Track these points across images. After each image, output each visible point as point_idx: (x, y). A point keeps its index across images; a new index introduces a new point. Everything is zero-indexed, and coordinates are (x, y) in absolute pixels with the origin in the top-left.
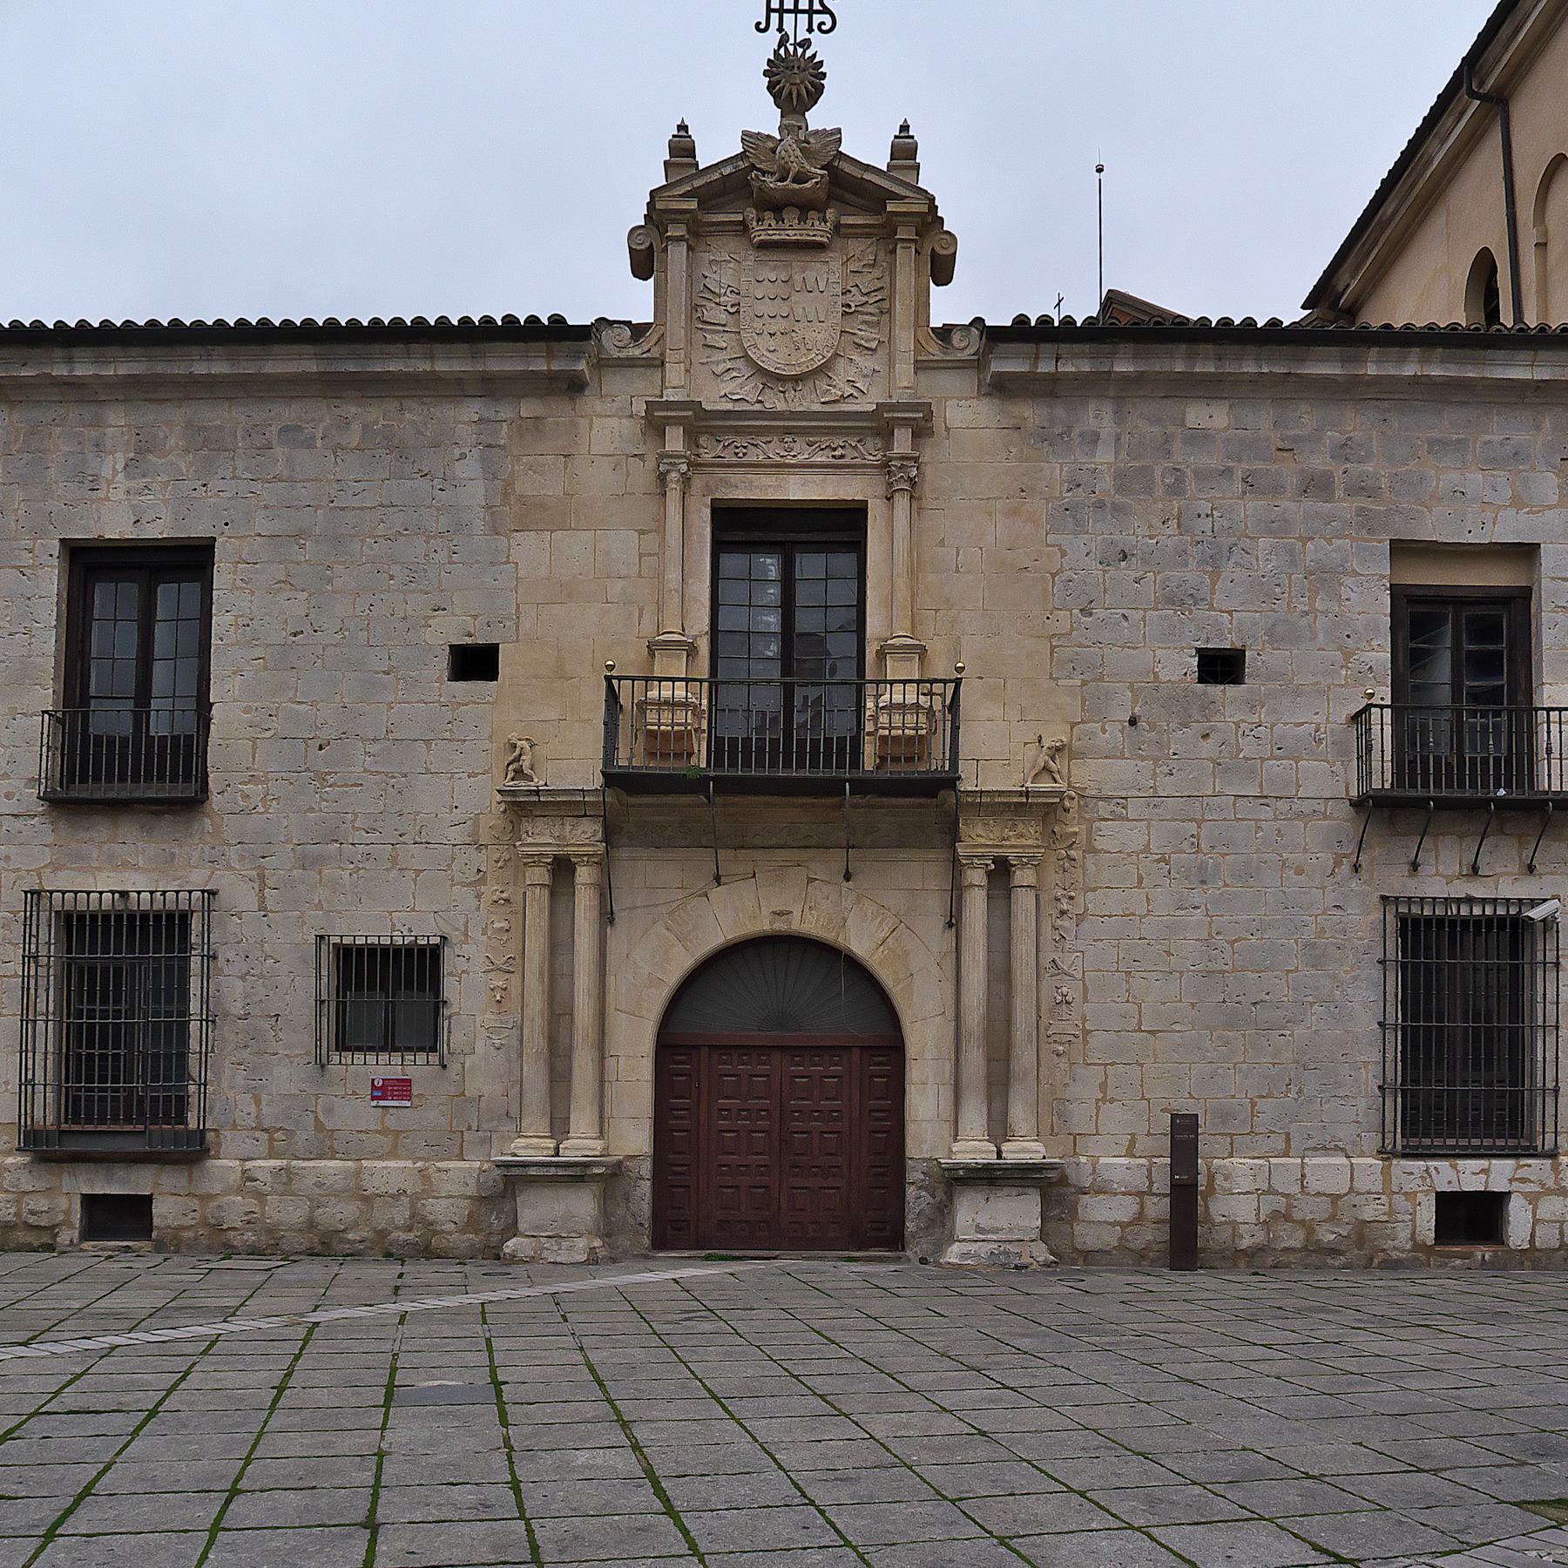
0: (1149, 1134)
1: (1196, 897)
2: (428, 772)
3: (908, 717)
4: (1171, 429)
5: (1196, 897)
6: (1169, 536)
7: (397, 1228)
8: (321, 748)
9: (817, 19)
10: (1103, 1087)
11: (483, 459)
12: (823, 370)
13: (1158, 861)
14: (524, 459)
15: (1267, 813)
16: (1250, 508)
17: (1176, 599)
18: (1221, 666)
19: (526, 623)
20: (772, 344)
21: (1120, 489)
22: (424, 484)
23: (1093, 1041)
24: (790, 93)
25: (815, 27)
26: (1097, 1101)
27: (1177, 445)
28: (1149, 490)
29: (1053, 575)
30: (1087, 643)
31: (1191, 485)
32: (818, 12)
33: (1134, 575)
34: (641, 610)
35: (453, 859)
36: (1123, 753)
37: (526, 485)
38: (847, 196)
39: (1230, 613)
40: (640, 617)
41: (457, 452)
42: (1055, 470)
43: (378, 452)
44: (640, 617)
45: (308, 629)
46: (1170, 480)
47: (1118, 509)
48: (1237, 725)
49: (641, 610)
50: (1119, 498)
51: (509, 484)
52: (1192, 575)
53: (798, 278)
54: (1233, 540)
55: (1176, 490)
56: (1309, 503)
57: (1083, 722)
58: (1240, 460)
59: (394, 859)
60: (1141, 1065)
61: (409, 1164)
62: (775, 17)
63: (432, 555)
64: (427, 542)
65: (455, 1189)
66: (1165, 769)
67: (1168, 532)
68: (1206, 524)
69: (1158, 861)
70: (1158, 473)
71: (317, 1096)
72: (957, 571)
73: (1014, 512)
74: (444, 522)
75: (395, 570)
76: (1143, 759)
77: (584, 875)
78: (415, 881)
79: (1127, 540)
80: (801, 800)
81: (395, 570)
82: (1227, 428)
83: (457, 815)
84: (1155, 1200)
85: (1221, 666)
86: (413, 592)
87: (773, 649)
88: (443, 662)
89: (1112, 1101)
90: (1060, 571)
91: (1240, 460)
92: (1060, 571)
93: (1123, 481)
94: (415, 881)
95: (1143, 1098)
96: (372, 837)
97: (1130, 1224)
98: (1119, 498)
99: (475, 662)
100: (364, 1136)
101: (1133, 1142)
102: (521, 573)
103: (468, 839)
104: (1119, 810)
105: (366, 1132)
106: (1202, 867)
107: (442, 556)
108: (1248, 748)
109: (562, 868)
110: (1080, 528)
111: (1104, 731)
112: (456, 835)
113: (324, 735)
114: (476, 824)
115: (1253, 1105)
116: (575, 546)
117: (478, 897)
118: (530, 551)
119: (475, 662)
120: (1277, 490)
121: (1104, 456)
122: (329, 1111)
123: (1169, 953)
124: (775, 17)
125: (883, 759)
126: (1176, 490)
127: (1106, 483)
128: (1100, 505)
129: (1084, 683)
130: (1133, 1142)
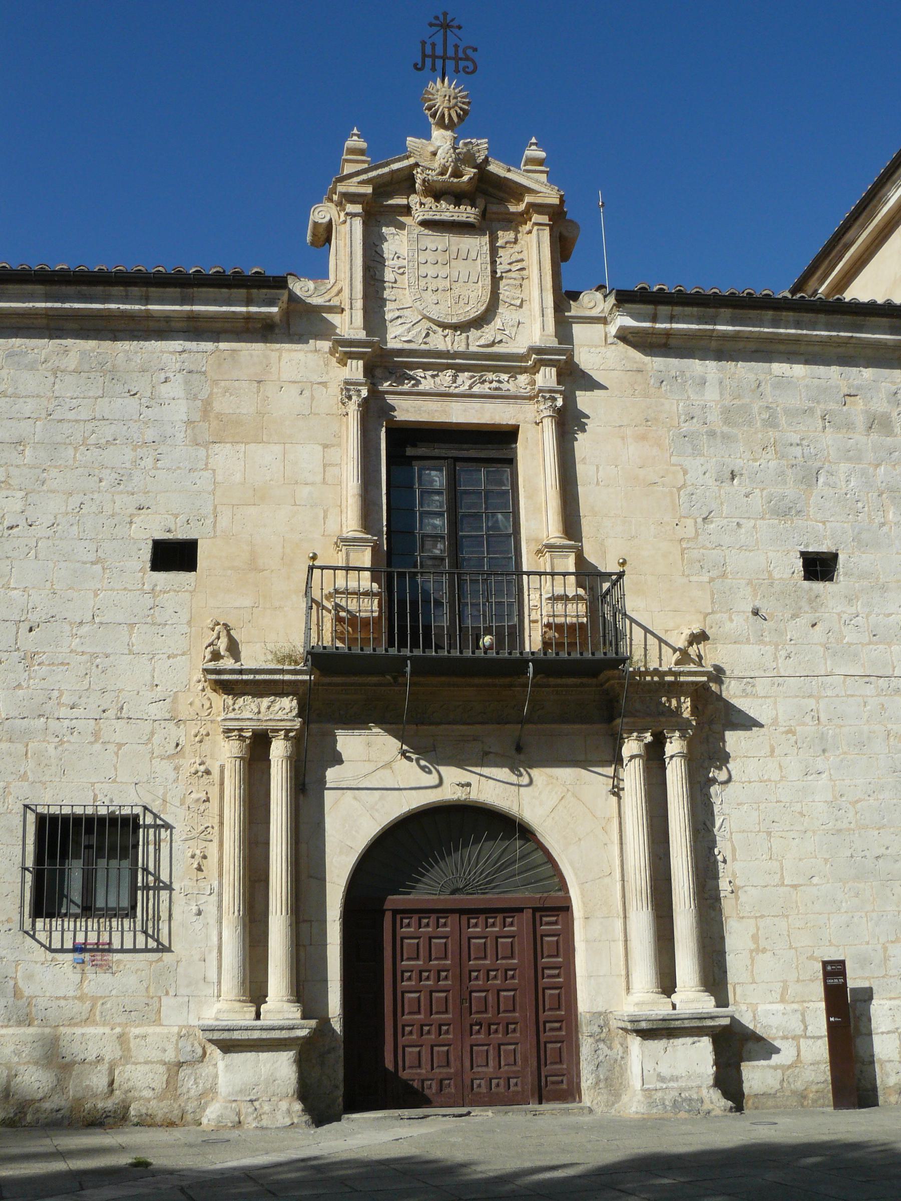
0: (798, 981)
1: (820, 764)
2: (131, 652)
3: (569, 606)
4: (761, 377)
5: (820, 764)
6: (770, 463)
7: (95, 1096)
8: (31, 630)
9: (462, 64)
10: (755, 938)
11: (187, 382)
12: (480, 322)
13: (787, 732)
14: (223, 384)
15: (869, 690)
16: (829, 440)
17: (784, 511)
18: (820, 567)
19: (224, 522)
20: (434, 298)
21: (727, 421)
22: (134, 401)
23: (743, 897)
24: (444, 115)
25: (461, 69)
26: (751, 951)
27: (767, 389)
28: (750, 423)
29: (679, 489)
30: (709, 546)
31: (783, 421)
32: (461, 59)
33: (744, 491)
34: (325, 512)
35: (153, 733)
36: (748, 640)
37: (222, 405)
38: (490, 190)
39: (824, 523)
40: (325, 517)
41: (162, 376)
42: (672, 405)
43: (92, 375)
44: (325, 517)
45: (23, 523)
46: (765, 416)
47: (726, 437)
48: (839, 614)
49: (325, 512)
50: (725, 429)
51: (207, 408)
52: (790, 490)
53: (454, 249)
54: (819, 464)
55: (771, 423)
56: (874, 436)
57: (713, 612)
58: (818, 402)
59: (96, 735)
60: (787, 916)
61: (107, 1030)
62: (428, 61)
63: (138, 461)
64: (134, 450)
65: (155, 1055)
66: (783, 653)
67: (769, 456)
68: (798, 451)
69: (787, 732)
70: (755, 409)
71: (17, 963)
72: (598, 483)
73: (643, 438)
74: (150, 434)
75: (105, 474)
76: (765, 644)
77: (279, 750)
78: (117, 754)
79: (738, 464)
80: (477, 681)
81: (105, 474)
82: (804, 378)
83: (159, 692)
84: (810, 1042)
85: (820, 567)
86: (121, 492)
87: (439, 549)
88: (146, 554)
89: (764, 951)
90: (684, 486)
91: (818, 402)
92: (684, 486)
93: (728, 415)
94: (117, 754)
95: (791, 947)
96: (76, 712)
97: (790, 1067)
98: (725, 429)
99: (175, 555)
100: (62, 1003)
101: (785, 989)
102: (219, 478)
103: (168, 716)
104: (749, 689)
105: (65, 998)
106: (822, 737)
107: (148, 462)
108: (850, 636)
109: (259, 743)
110: (696, 452)
111: (731, 620)
112: (156, 711)
113: (34, 617)
114: (175, 700)
115: (885, 949)
116: (265, 457)
117: (177, 768)
118: (225, 458)
119: (175, 555)
120: (849, 426)
121: (711, 394)
122: (30, 977)
123: (802, 815)
124: (428, 61)
125: (546, 644)
126: (771, 423)
127: (714, 417)
128: (712, 434)
129: (712, 580)
130: (785, 989)
